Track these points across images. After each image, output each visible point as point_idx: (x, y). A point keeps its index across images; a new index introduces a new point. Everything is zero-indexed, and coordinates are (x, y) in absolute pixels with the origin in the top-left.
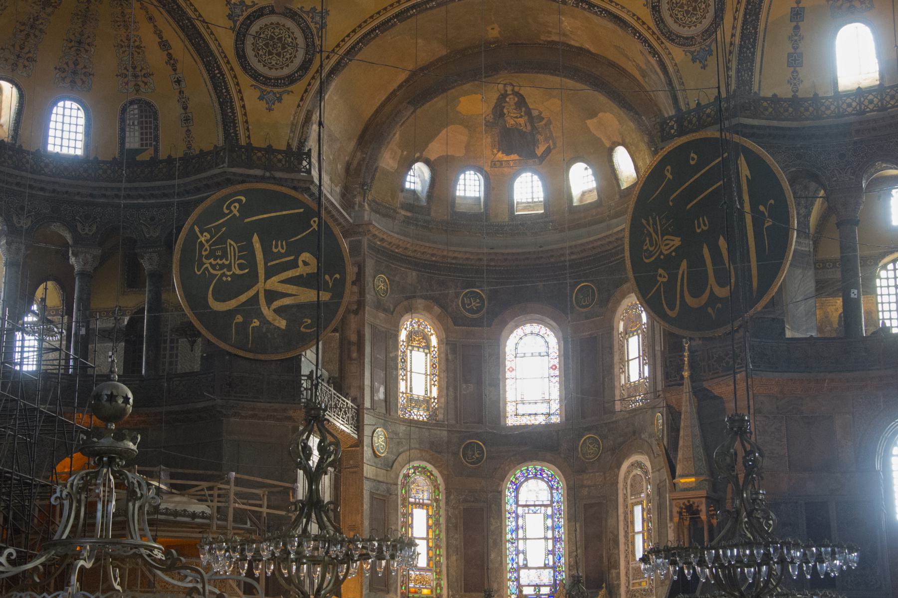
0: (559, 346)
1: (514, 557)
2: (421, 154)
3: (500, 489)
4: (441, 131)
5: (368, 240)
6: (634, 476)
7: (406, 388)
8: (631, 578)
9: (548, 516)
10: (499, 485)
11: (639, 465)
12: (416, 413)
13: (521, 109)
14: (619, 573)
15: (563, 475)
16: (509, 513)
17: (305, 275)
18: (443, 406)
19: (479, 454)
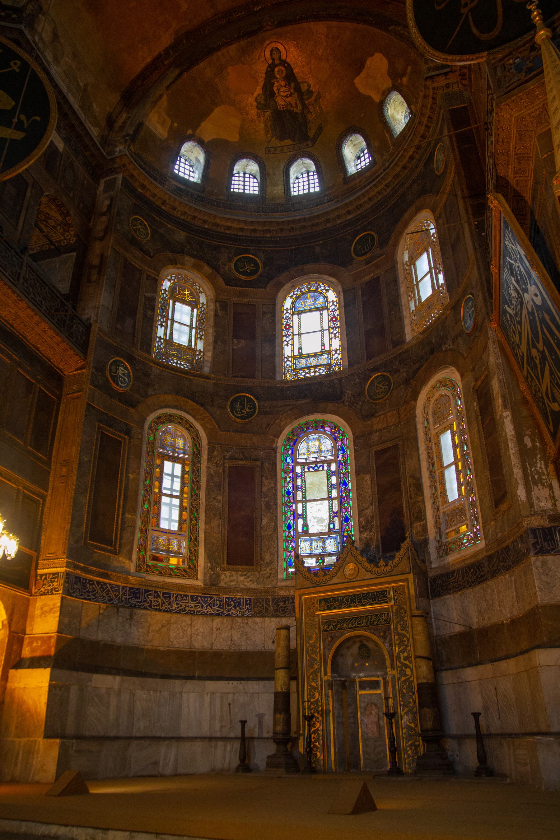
0: (339, 299)
1: (292, 522)
3: (274, 446)
4: (212, 111)
5: (123, 178)
6: (437, 400)
7: (165, 334)
8: (443, 527)
9: (333, 474)
10: (273, 441)
11: (443, 383)
12: (175, 361)
14: (425, 525)
15: (348, 424)
16: (286, 473)
19: (250, 408)
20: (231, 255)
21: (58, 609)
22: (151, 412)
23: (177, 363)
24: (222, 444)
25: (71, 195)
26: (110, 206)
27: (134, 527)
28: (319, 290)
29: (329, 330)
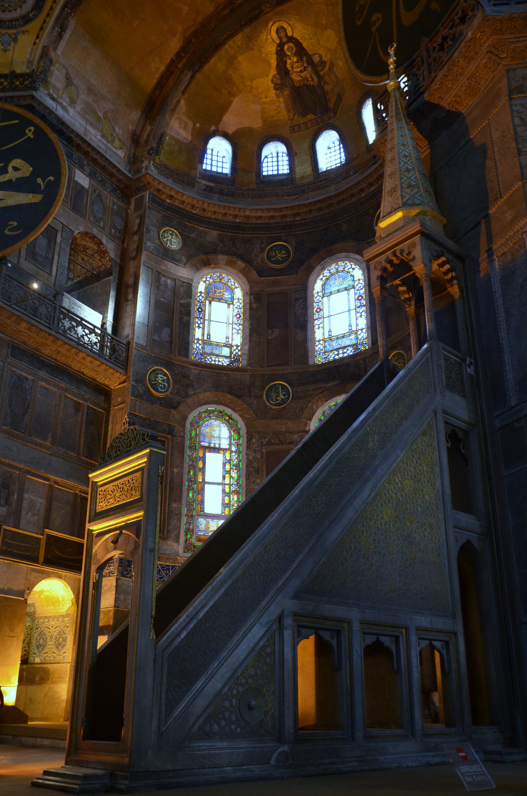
0: (364, 277)
2: (217, 126)
3: (307, 429)
4: (231, 102)
10: (306, 424)
12: (213, 359)
13: (302, 60)
17: (14, 180)
18: (247, 352)
19: (284, 395)
20: (263, 245)
21: (114, 588)
22: (192, 410)
23: (215, 361)
24: (259, 432)
25: (102, 225)
26: (140, 225)
27: (180, 514)
28: (346, 269)
29: (355, 309)
